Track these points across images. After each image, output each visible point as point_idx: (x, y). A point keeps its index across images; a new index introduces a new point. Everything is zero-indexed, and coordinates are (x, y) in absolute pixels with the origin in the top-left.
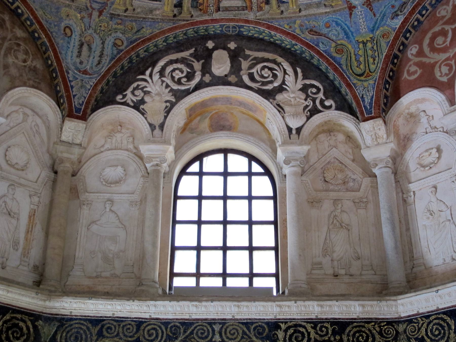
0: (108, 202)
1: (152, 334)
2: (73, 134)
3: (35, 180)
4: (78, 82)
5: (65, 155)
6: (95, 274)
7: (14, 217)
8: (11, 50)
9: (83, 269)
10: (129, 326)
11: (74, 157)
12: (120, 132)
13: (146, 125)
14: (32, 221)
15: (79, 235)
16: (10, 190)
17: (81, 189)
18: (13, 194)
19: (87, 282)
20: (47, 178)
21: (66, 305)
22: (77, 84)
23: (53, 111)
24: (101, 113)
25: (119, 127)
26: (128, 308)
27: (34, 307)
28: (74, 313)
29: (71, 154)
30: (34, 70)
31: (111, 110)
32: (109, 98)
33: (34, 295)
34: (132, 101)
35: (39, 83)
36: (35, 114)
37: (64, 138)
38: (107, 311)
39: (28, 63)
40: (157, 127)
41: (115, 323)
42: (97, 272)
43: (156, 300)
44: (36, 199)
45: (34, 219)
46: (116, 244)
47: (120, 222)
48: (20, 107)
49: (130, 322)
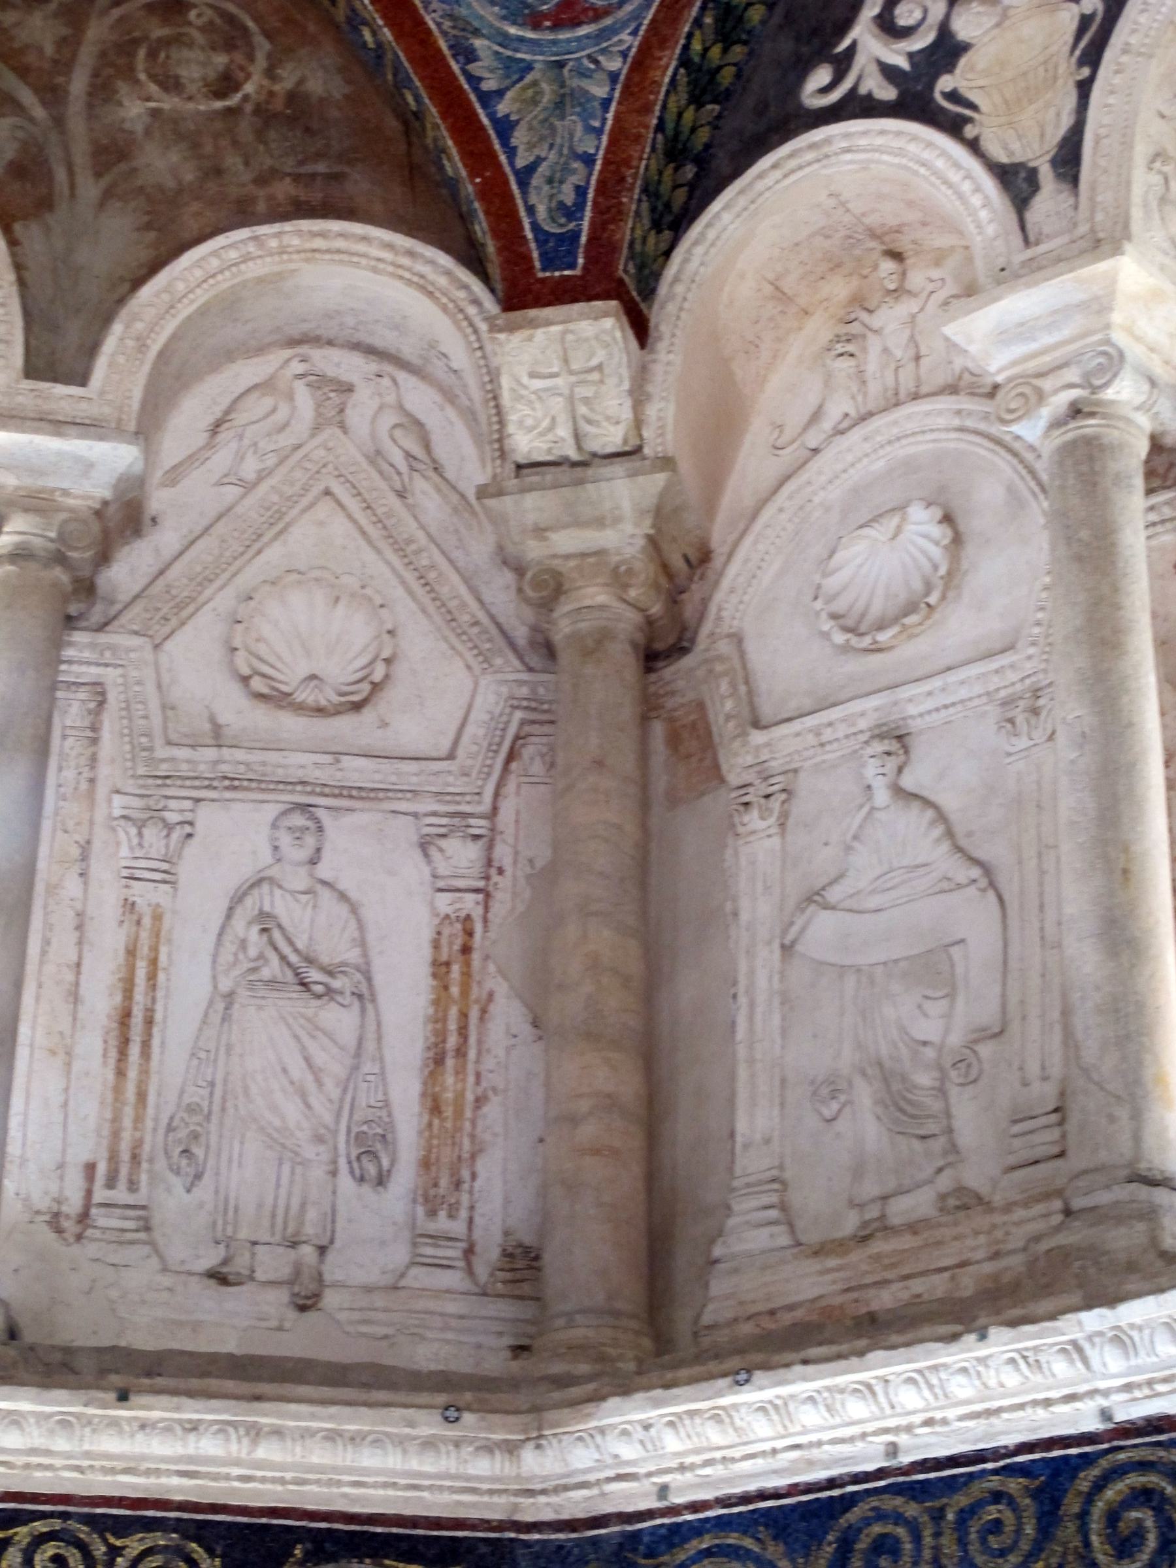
0: (869, 751)
1: (1139, 1533)
2: (571, 400)
3: (445, 745)
4: (535, 83)
5: (566, 541)
6: (850, 1224)
7: (330, 992)
8: (132, 55)
9: (783, 1207)
10: (992, 1512)
11: (625, 539)
12: (899, 292)
13: (977, 189)
14: (455, 990)
15: (743, 1000)
16: (285, 840)
17: (728, 718)
18: (313, 862)
19: (808, 1284)
20: (519, 715)
21: (628, 1451)
22: (534, 102)
23: (444, 309)
24: (726, 217)
25: (888, 266)
26: (961, 1388)
27: (447, 1497)
28: (682, 1490)
29: (599, 522)
30: (297, 113)
31: (777, 174)
32: (761, 109)
33: (429, 1425)
34: (889, 72)
35: (336, 178)
36: (388, 368)
37: (526, 444)
38: (851, 1440)
39: (249, 88)
40: (1046, 174)
41: (912, 1510)
42: (861, 1206)
43: (1112, 1300)
44: (462, 855)
45: (467, 974)
46: (951, 996)
47: (959, 849)
48: (288, 353)
49: (994, 1482)
